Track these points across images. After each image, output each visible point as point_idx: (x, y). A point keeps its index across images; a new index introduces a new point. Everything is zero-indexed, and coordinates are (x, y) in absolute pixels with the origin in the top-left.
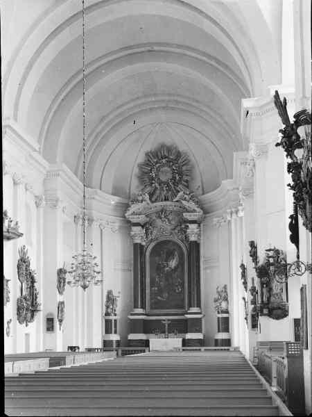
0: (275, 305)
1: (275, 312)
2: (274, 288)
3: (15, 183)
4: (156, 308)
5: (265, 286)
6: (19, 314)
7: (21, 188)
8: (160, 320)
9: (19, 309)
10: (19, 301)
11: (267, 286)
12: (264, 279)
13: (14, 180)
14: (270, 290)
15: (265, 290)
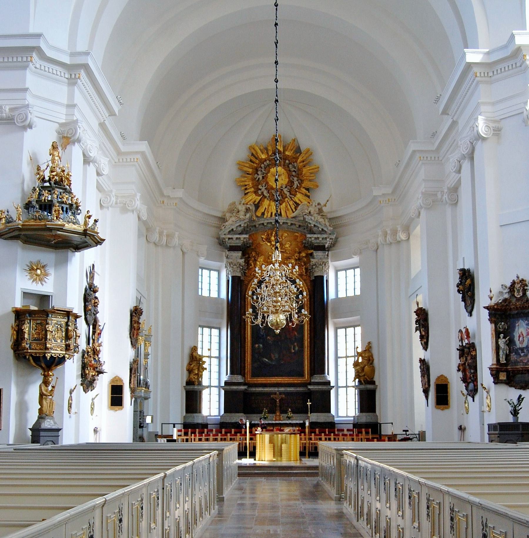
0: (520, 366)
1: (519, 377)
2: (516, 339)
3: (87, 160)
4: (258, 376)
5: (502, 335)
6: (84, 375)
7: (91, 169)
8: (269, 394)
9: (84, 367)
10: (84, 352)
11: (504, 338)
12: (502, 325)
13: (84, 155)
14: (511, 343)
15: (502, 342)
